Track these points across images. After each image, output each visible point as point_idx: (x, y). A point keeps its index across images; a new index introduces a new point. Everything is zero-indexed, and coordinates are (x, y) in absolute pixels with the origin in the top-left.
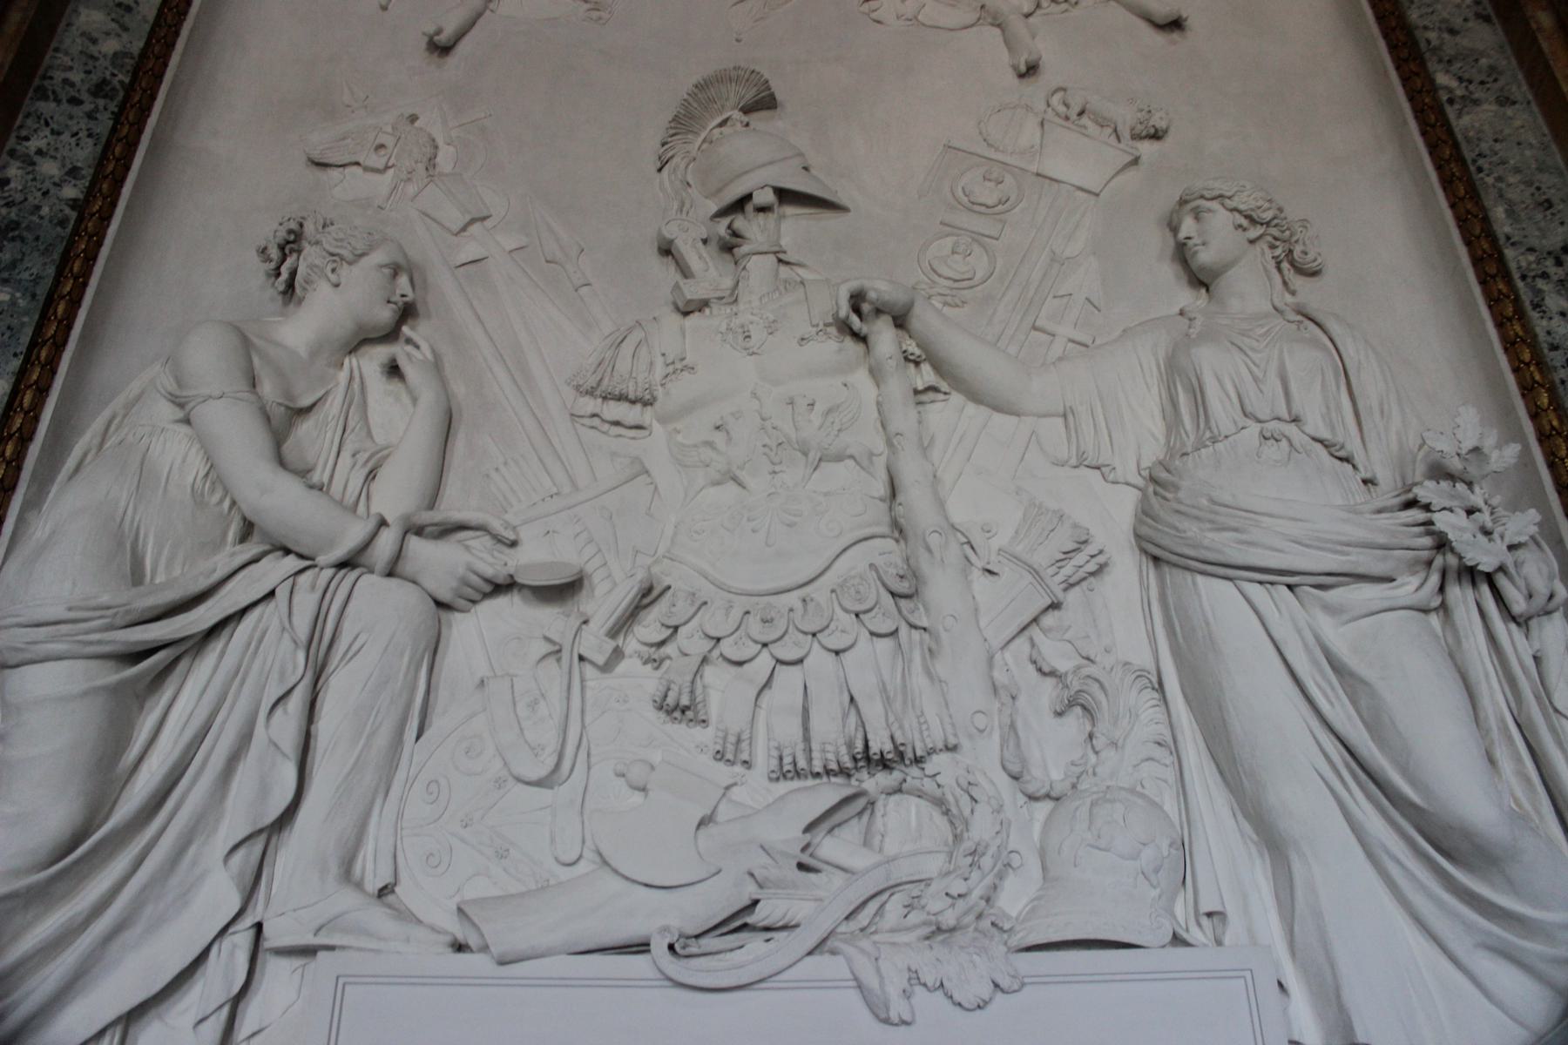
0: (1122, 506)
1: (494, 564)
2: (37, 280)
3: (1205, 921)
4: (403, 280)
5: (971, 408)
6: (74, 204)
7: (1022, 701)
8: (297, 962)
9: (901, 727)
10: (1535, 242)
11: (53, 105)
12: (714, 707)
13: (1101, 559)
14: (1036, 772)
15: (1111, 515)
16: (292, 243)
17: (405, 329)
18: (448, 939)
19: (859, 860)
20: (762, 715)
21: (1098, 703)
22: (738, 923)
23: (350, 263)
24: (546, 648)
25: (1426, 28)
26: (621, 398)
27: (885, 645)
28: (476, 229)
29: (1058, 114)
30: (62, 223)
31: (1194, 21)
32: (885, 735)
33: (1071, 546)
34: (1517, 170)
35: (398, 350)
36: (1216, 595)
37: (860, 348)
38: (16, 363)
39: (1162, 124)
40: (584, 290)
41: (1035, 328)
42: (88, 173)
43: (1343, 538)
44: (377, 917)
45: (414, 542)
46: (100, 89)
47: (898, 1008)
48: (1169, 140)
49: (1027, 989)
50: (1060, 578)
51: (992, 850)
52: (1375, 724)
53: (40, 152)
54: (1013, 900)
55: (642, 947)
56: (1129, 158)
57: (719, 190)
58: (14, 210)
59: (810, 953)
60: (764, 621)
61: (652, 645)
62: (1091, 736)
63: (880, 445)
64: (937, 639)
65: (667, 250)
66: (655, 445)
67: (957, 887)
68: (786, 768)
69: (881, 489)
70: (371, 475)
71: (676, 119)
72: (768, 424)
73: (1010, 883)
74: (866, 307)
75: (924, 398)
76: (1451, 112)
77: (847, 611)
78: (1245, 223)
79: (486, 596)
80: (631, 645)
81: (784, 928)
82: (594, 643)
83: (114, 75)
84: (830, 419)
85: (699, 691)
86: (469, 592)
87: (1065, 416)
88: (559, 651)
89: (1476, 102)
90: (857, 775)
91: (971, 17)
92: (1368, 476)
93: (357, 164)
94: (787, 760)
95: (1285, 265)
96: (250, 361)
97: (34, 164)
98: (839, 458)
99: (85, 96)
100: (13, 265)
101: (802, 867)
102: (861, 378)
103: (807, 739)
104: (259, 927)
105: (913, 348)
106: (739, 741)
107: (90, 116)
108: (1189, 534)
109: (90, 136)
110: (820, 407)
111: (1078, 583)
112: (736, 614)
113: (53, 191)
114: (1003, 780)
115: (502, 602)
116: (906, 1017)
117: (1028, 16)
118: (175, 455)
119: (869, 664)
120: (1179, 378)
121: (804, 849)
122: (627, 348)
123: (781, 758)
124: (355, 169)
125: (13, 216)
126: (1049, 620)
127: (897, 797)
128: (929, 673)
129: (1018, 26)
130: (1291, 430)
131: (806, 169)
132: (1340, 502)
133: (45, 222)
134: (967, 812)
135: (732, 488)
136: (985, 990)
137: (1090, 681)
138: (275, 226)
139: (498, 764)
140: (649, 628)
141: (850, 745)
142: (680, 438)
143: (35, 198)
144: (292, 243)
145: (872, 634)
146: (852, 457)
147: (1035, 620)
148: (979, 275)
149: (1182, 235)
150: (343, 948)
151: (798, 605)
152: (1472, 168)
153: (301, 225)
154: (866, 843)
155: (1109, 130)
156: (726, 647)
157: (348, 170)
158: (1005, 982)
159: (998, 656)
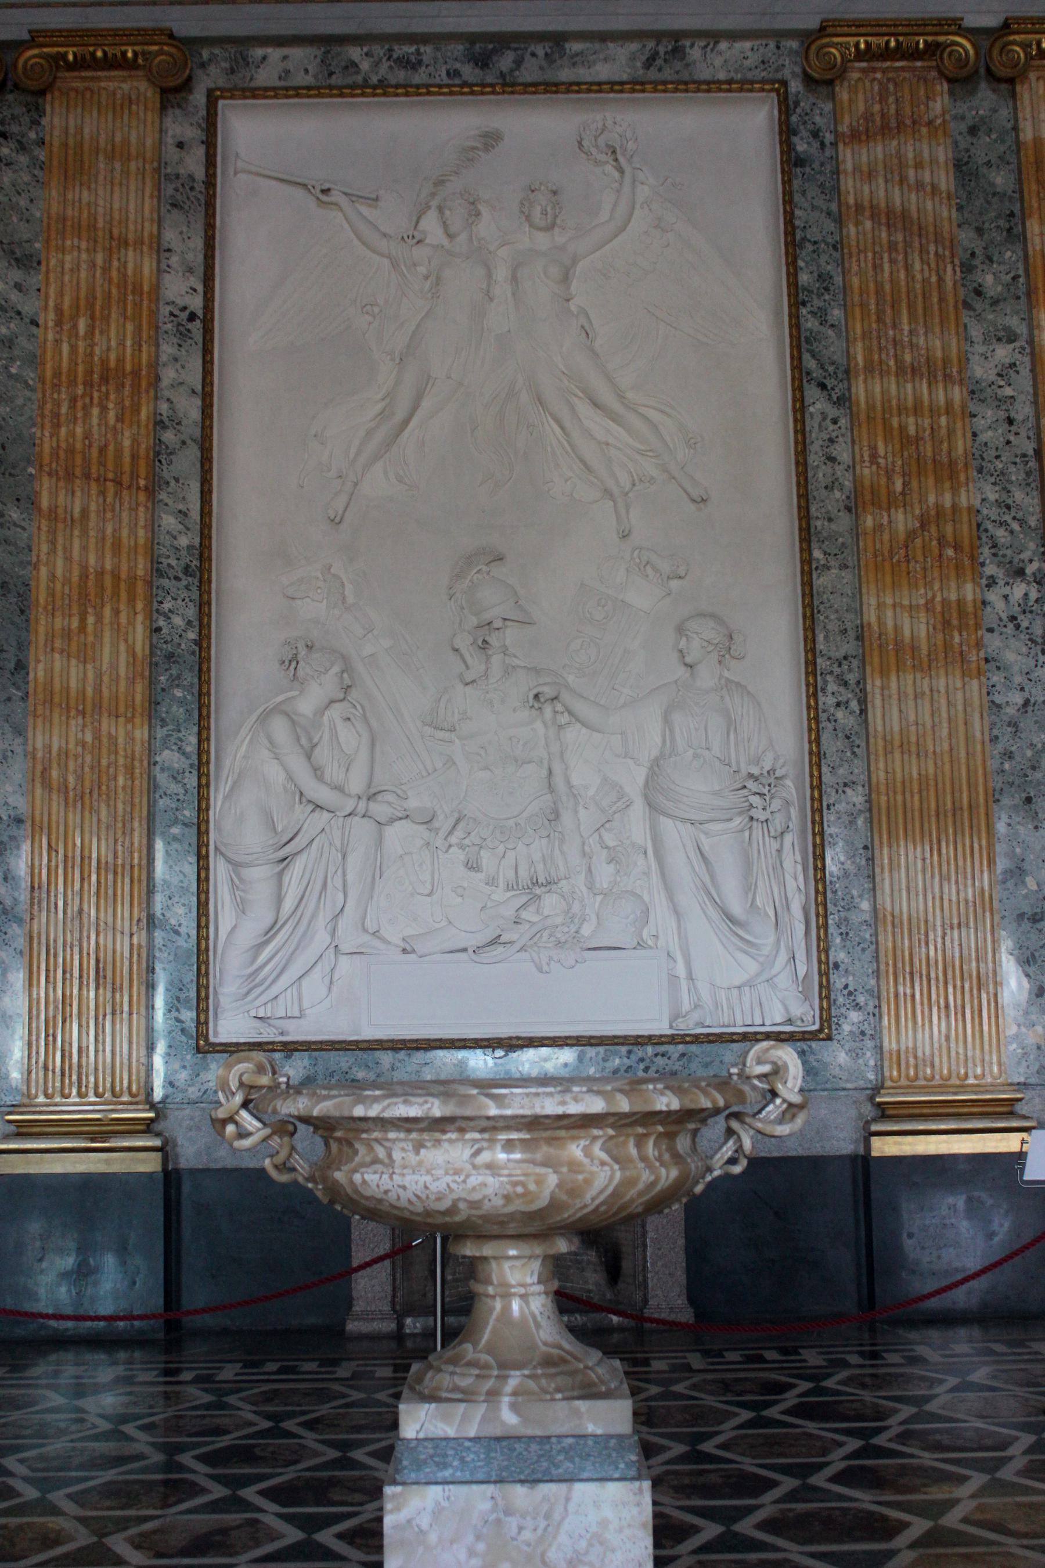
0: (641, 775)
2: (192, 685)
4: (345, 675)
5: (584, 730)
10: (832, 654)
12: (484, 862)
14: (598, 886)
15: (633, 778)
16: (295, 659)
22: (495, 941)
27: (544, 841)
30: (193, 653)
34: (837, 611)
36: (667, 825)
38: (196, 729)
42: (196, 623)
46: (187, 568)
47: (545, 968)
54: (586, 930)
55: (464, 950)
67: (566, 930)
69: (545, 772)
73: (585, 926)
76: (814, 576)
80: (453, 839)
82: (439, 842)
89: (828, 568)
99: (181, 575)
100: (178, 677)
107: (187, 587)
114: (584, 889)
118: (274, 773)
120: (667, 720)
126: (607, 826)
136: (573, 962)
143: (177, 640)
154: (538, 912)
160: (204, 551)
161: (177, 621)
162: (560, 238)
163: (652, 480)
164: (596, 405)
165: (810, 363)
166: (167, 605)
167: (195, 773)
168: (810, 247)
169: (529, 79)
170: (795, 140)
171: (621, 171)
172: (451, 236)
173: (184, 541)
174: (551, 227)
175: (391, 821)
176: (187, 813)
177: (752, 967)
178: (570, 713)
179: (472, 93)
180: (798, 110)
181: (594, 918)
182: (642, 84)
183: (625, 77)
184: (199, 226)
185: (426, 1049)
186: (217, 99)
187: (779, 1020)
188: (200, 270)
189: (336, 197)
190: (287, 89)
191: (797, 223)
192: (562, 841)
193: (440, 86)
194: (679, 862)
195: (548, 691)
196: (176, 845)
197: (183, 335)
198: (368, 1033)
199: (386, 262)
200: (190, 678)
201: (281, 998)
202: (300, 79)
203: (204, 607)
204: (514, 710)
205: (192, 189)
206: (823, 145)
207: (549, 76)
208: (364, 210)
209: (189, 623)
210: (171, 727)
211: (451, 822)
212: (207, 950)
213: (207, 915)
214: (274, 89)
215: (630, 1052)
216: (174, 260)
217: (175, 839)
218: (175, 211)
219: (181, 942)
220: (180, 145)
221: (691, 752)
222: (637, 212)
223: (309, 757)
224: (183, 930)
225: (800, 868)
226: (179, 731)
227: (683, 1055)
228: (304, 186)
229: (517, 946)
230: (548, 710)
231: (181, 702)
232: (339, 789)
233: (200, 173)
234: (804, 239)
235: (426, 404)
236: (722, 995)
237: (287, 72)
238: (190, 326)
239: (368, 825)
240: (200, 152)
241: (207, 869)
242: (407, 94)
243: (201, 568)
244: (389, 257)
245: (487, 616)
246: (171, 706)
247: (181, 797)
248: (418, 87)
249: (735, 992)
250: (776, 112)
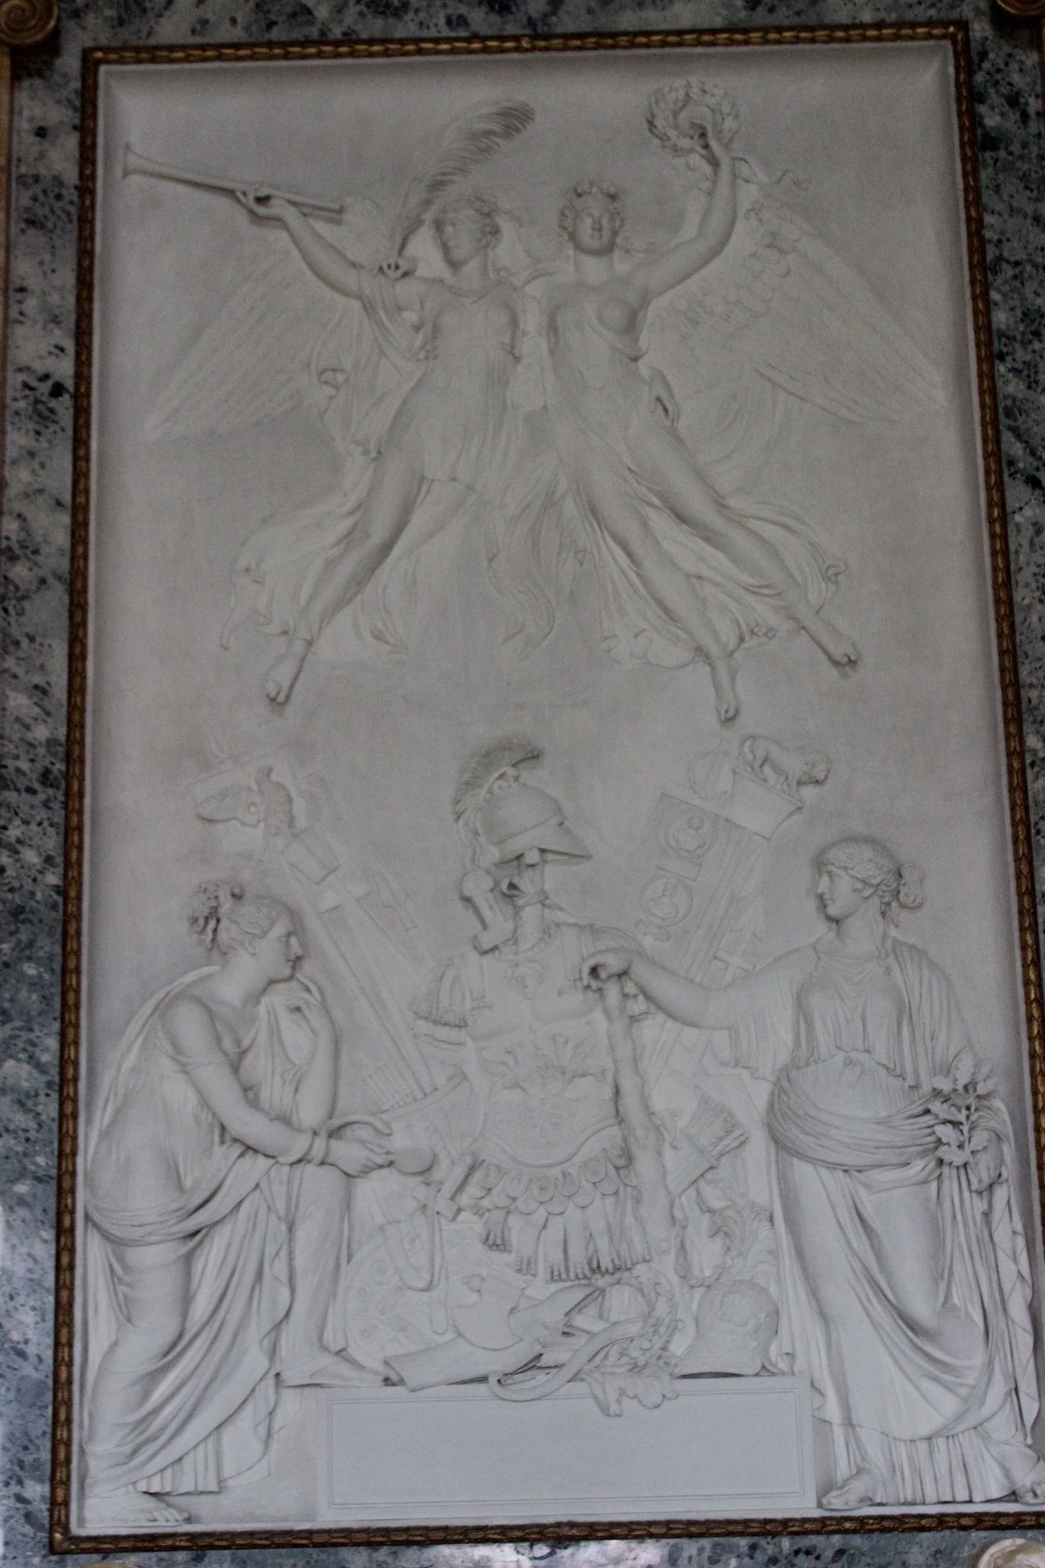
0: (761, 1093)
2: (51, 957)
3: (785, 1357)
4: (293, 940)
5: (670, 1024)
6: (58, 890)
7: (690, 1228)
8: (299, 1390)
9: (619, 1256)
11: (15, 794)
12: (514, 1238)
13: (742, 1139)
14: (696, 1272)
16: (214, 915)
17: (299, 976)
18: (380, 1378)
19: (596, 1327)
20: (541, 1245)
22: (532, 1365)
23: (261, 938)
25: (1031, 686)
27: (610, 1201)
30: (54, 907)
32: (609, 1259)
33: (721, 1133)
38: (57, 1026)
41: (716, 958)
42: (59, 860)
44: (344, 1369)
46: (45, 777)
47: (614, 1408)
48: (829, 781)
51: (666, 1322)
52: (879, 1256)
53: (19, 841)
54: (679, 1346)
55: (483, 1379)
56: (793, 808)
58: (16, 895)
59: (569, 1381)
60: (541, 1189)
63: (608, 1064)
67: (646, 1345)
69: (608, 1092)
73: (677, 1337)
76: (1030, 774)
78: (860, 886)
79: (374, 1169)
80: (465, 1199)
81: (556, 1367)
82: (442, 1204)
83: (52, 764)
92: (913, 1083)
93: (236, 819)
97: (17, 852)
98: (584, 1075)
99: (37, 786)
100: (31, 944)
101: (564, 1333)
102: (598, 1016)
103: (566, 1259)
104: (278, 1375)
106: (529, 1263)
107: (46, 805)
108: (789, 1135)
109: (51, 825)
110: (571, 1044)
111: (729, 1152)
113: (39, 877)
114: (675, 1280)
115: (385, 1171)
116: (618, 1413)
123: (552, 1272)
125: (18, 901)
126: (709, 1176)
130: (864, 1057)
133: (42, 907)
134: (654, 1299)
136: (658, 1399)
141: (590, 1263)
142: (484, 1053)
143: (28, 886)
145: (603, 1195)
146: (591, 1074)
147: (702, 1175)
151: (560, 1176)
152: (1033, 831)
154: (600, 1316)
158: (669, 1395)
159: (677, 1200)
160: (72, 750)
161: (31, 856)
162: (621, 265)
163: (770, 633)
164: (680, 517)
165: (1014, 448)
166: (14, 832)
167: (55, 1096)
168: (1009, 271)
169: (571, 28)
170: (982, 109)
171: (715, 163)
172: (454, 265)
173: (41, 733)
174: (608, 250)
175: (366, 1171)
176: (41, 1160)
177: (950, 1405)
179: (486, 50)
180: (986, 65)
181: (691, 1324)
182: (745, 31)
183: (718, 22)
184: (69, 254)
185: (422, 1544)
186: (98, 62)
187: (996, 1495)
188: (70, 320)
189: (278, 208)
190: (203, 47)
191: (988, 234)
192: (638, 1201)
193: (437, 41)
194: (827, 1236)
195: (613, 963)
196: (22, 1212)
197: (44, 417)
198: (329, 1518)
199: (356, 305)
200: (48, 946)
201: (188, 1462)
202: (225, 33)
203: (71, 834)
204: (560, 993)
205: (59, 197)
206: (1025, 117)
207: (604, 23)
208: (320, 226)
209: (49, 860)
210: (17, 1023)
211: (459, 1173)
212: (70, 1382)
213: (70, 1325)
214: (183, 48)
215: (753, 1547)
216: (31, 304)
217: (22, 1201)
218: (32, 231)
219: (27, 1369)
220: (41, 133)
221: (840, 1056)
222: (740, 226)
223: (236, 1069)
224: (31, 1350)
225: (1021, 1242)
226: (31, 1030)
227: (840, 1553)
228: (230, 192)
230: (613, 991)
231: (35, 984)
232: (285, 1120)
233: (70, 174)
234: (999, 259)
235: (419, 520)
236: (902, 1452)
237: (204, 22)
238: (53, 403)
239: (329, 1178)
240: (71, 142)
241: (72, 1251)
242: (386, 54)
243: (67, 776)
244: (360, 297)
245: (516, 845)
246: (18, 991)
247: (33, 1135)
248: (402, 42)
249: (923, 1447)
250: (951, 70)
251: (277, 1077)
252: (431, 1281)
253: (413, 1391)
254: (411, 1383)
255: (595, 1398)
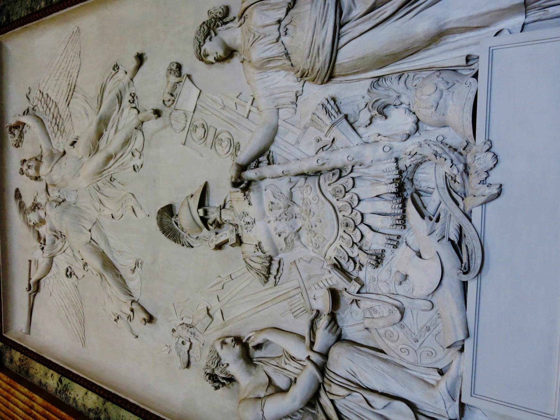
1: (323, 322)
5: (275, 143)
21: (383, 103)
22: (457, 246)
23: (221, 359)
24: (354, 305)
26: (269, 268)
27: (357, 182)
28: (211, 312)
29: (173, 104)
31: (139, 50)
35: (251, 345)
36: (344, 56)
37: (253, 183)
39: (175, 65)
40: (233, 277)
41: (247, 118)
43: (322, 6)
45: (316, 348)
49: (490, 139)
50: (336, 115)
54: (456, 140)
56: (187, 79)
57: (199, 227)
61: (355, 266)
62: (395, 105)
63: (286, 179)
64: (356, 163)
65: (219, 247)
66: (287, 257)
68: (400, 223)
69: (302, 179)
70: (293, 358)
71: (175, 241)
72: (278, 219)
74: (239, 181)
75: (271, 160)
77: (344, 196)
78: (209, 38)
79: (336, 323)
80: (355, 274)
82: (354, 287)
84: (277, 196)
85: (371, 252)
86: (335, 328)
87: (278, 109)
88: (356, 300)
90: (405, 195)
91: (140, 133)
94: (397, 222)
95: (224, 20)
96: (251, 398)
98: (291, 194)
101: (437, 220)
102: (264, 184)
105: (253, 164)
106: (390, 239)
112: (345, 236)
114: (409, 141)
115: (338, 317)
117: (139, 112)
119: (364, 189)
120: (265, 65)
121: (431, 219)
122: (252, 264)
123: (397, 224)
124: (190, 352)
126: (352, 120)
127: (414, 181)
128: (369, 166)
129: (141, 116)
130: (283, 23)
131: (192, 196)
132: (309, 6)
134: (420, 156)
135: (300, 232)
136: (490, 155)
137: (374, 106)
138: (208, 383)
139: (395, 326)
140: (349, 267)
144: (213, 378)
145: (353, 187)
146: (291, 189)
147: (351, 125)
148: (228, 136)
149: (213, 61)
150: (461, 392)
153: (207, 374)
155: (178, 85)
156: (357, 240)
157: (191, 355)
158: (487, 147)
159: (364, 139)
178: (261, 153)
229: (465, 222)
251: (287, 367)
252: (396, 307)
253: (468, 336)
254: (461, 337)
255: (485, 203)
